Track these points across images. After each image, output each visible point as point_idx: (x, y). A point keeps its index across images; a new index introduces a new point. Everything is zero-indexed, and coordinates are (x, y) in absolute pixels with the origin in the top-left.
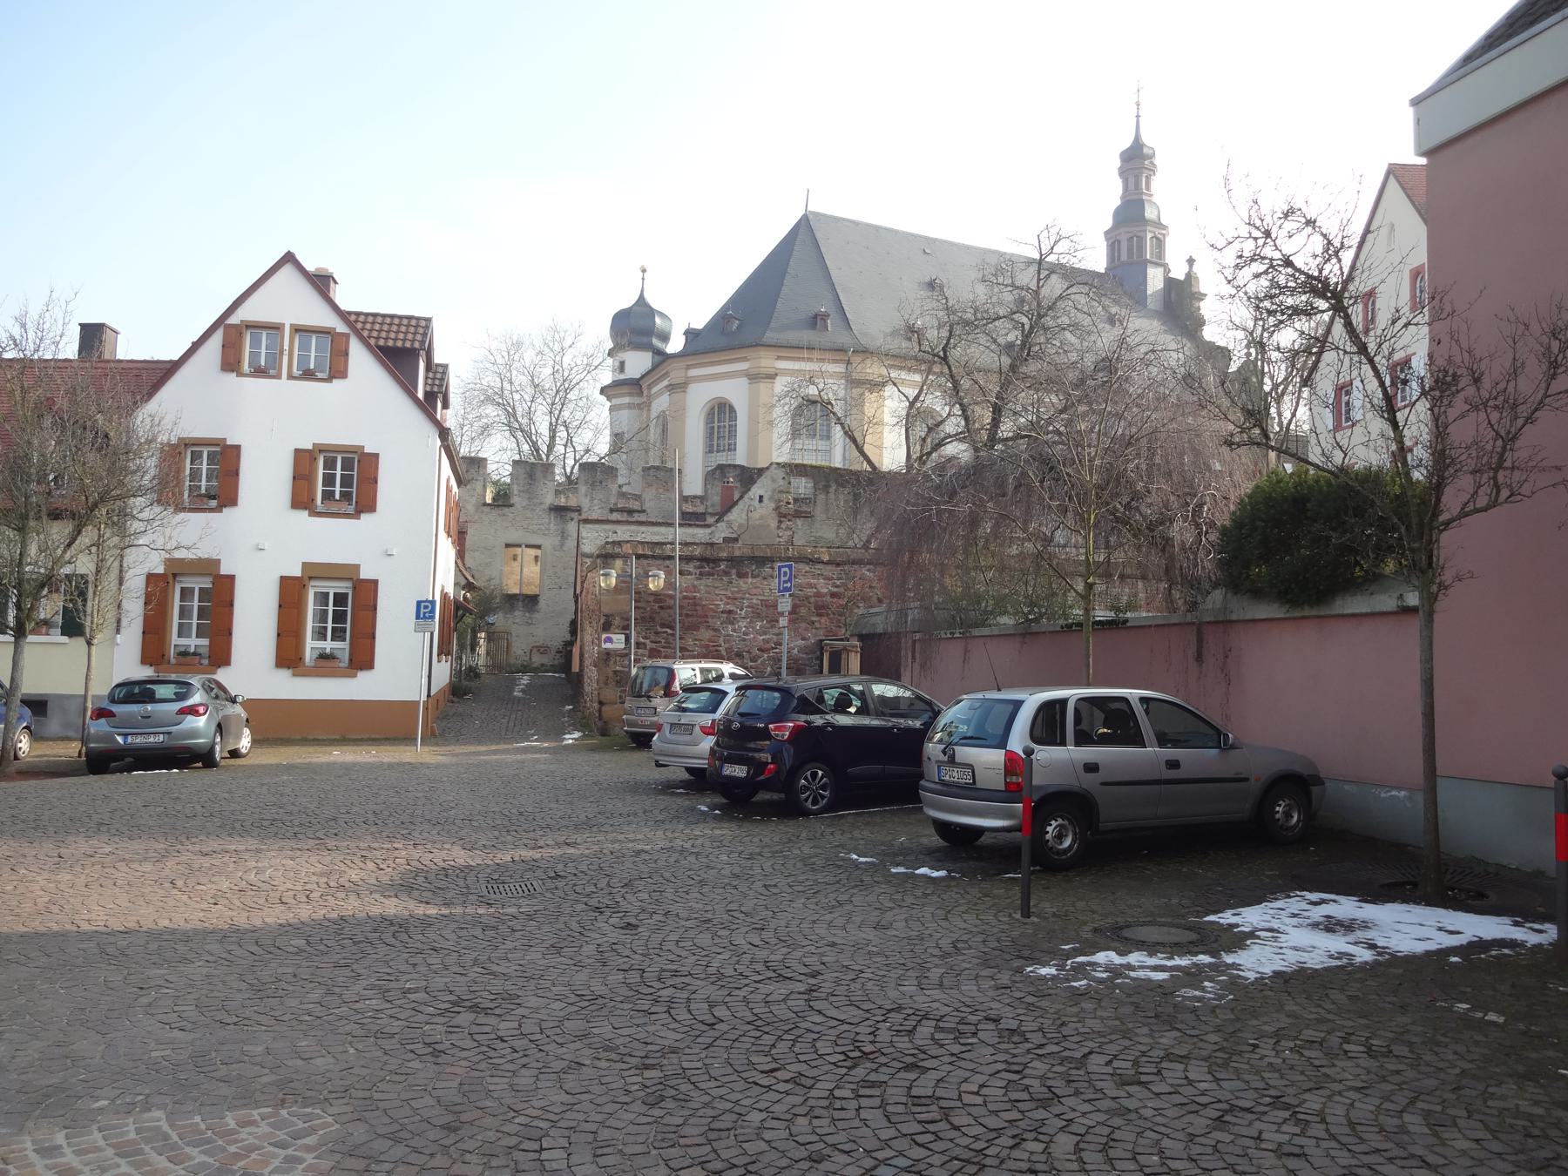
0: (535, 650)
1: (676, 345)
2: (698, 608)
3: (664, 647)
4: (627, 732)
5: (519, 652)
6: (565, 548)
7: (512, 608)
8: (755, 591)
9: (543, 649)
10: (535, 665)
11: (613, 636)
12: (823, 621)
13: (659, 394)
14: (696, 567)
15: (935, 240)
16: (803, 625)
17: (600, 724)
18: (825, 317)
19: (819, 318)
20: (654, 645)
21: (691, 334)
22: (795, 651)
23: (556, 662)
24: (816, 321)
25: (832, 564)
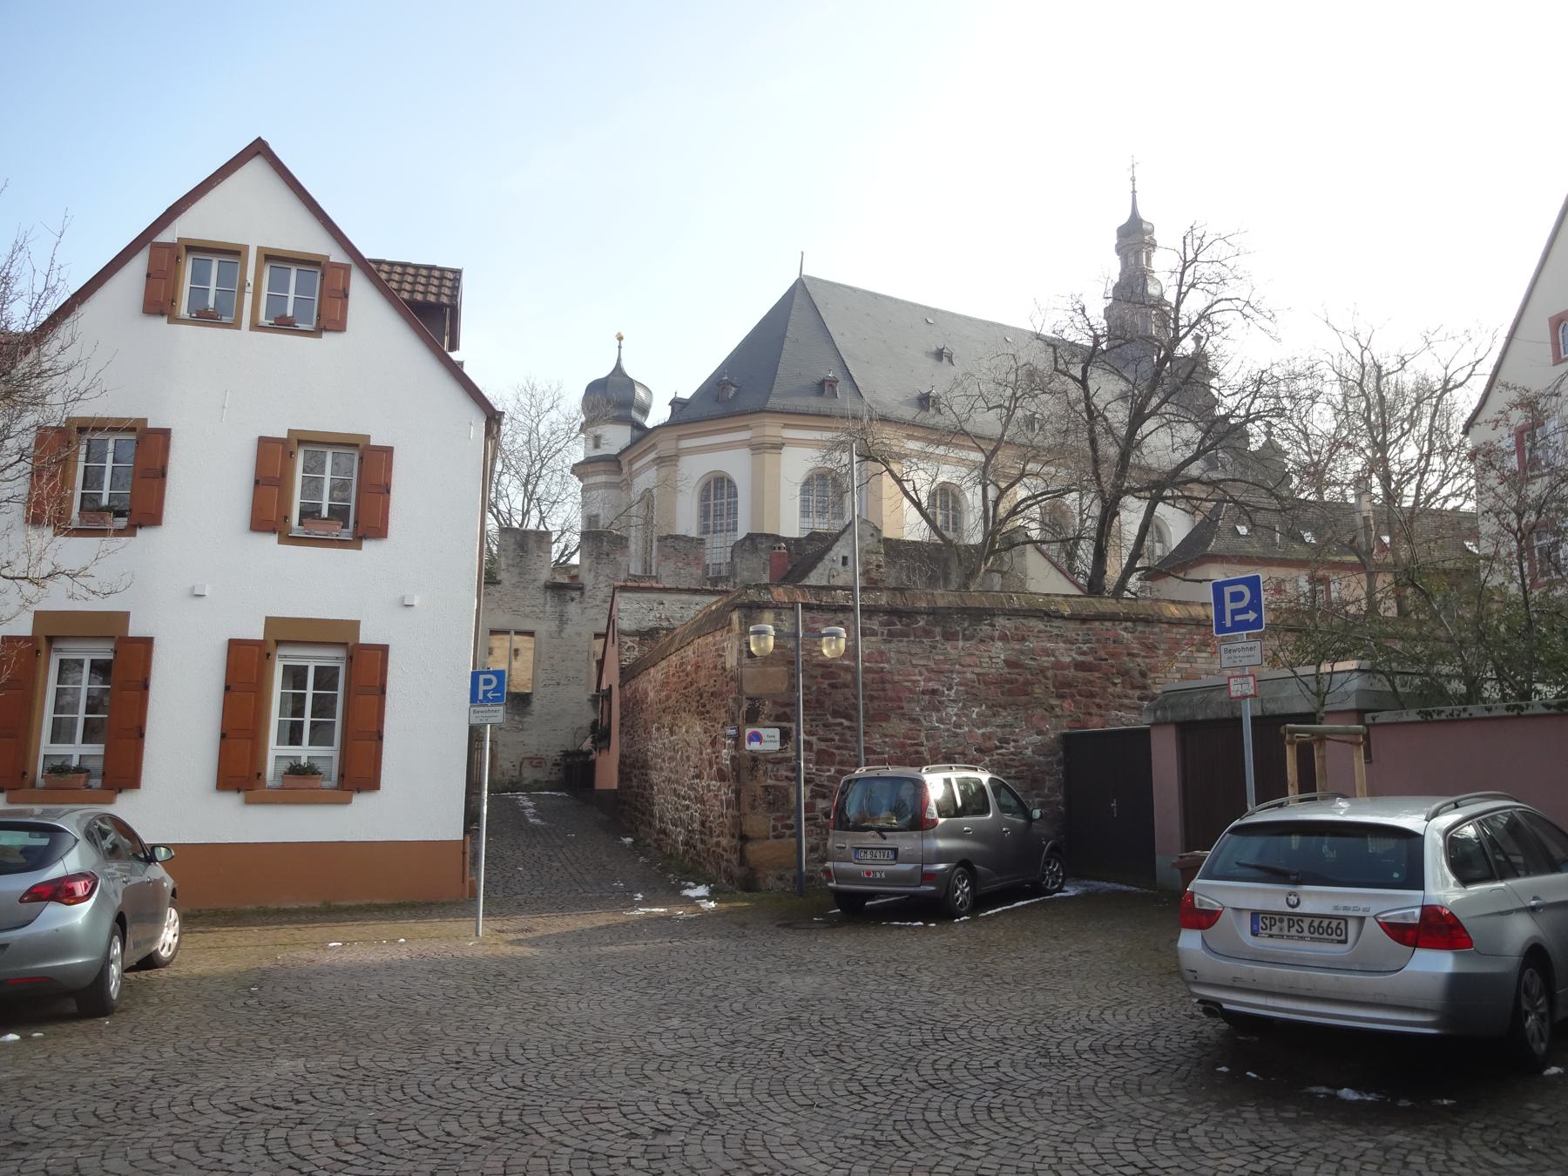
1: (658, 414)
2: (888, 686)
3: (838, 748)
4: (832, 890)
6: (563, 635)
8: (968, 660)
9: (536, 762)
10: (526, 782)
11: (761, 731)
12: (1066, 705)
13: (646, 467)
14: (882, 624)
15: (935, 311)
16: (1039, 711)
17: (738, 871)
18: (833, 383)
19: (827, 384)
20: (823, 745)
21: (676, 404)
22: (1029, 752)
23: (553, 778)
24: (824, 387)
25: (1076, 619)
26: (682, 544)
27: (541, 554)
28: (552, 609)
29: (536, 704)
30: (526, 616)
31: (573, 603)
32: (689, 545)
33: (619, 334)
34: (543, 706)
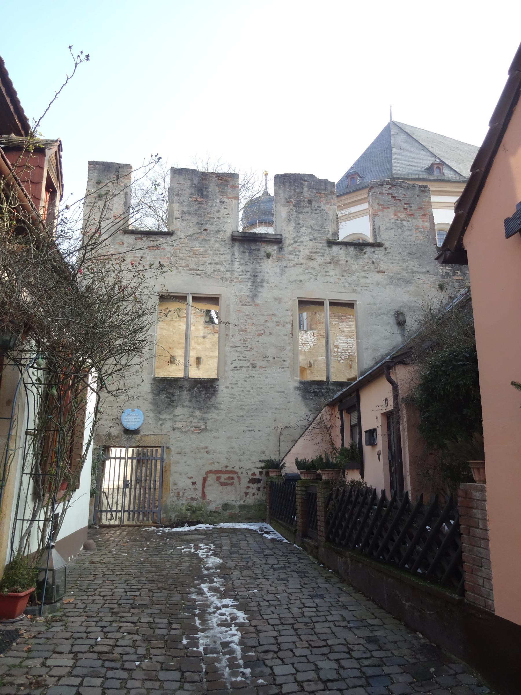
0: (211, 478)
5: (184, 483)
6: (258, 301)
7: (171, 403)
10: (212, 507)
19: (435, 167)
23: (250, 500)
26: (401, 191)
27: (225, 200)
28: (242, 268)
29: (222, 389)
30: (208, 276)
31: (270, 261)
32: (409, 193)
33: (265, 171)
34: (233, 397)
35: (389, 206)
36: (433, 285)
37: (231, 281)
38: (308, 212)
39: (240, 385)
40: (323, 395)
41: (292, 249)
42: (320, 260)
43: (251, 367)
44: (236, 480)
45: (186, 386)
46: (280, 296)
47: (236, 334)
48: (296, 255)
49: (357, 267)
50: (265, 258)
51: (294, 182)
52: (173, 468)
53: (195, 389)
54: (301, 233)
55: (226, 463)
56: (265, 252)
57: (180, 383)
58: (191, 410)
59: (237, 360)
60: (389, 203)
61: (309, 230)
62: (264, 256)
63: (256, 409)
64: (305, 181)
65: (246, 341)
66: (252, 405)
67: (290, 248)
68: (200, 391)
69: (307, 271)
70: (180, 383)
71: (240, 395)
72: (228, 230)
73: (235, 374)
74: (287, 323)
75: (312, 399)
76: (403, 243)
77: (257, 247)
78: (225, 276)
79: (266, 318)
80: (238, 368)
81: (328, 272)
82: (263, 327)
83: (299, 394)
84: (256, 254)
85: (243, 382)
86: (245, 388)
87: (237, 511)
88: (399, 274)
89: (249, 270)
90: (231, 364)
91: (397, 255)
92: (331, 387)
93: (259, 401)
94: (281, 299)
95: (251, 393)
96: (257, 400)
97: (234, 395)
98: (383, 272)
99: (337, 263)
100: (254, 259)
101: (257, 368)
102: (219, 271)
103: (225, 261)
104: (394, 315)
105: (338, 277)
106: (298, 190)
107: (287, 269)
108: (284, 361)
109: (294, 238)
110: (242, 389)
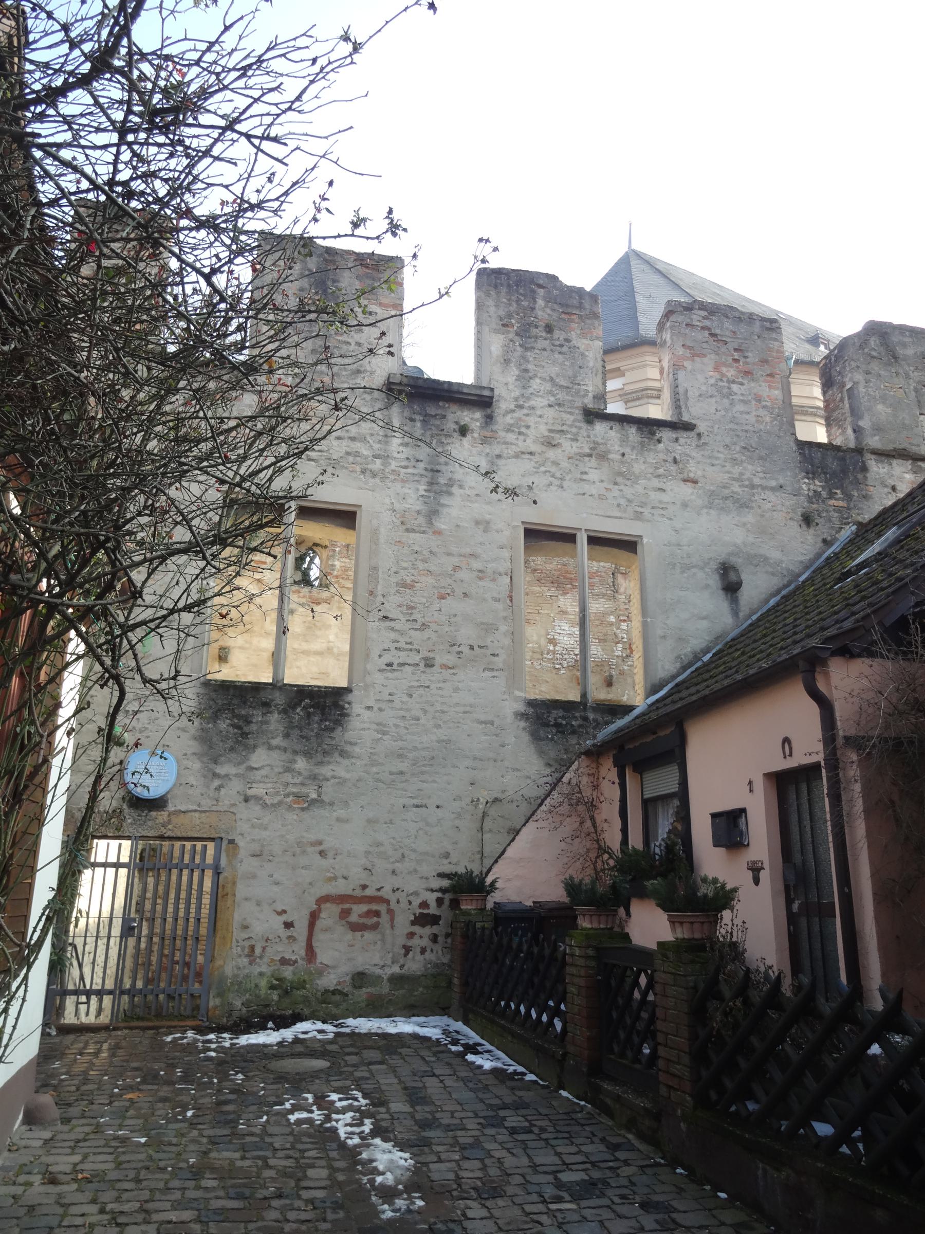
0: (329, 914)
10: (329, 981)
23: (415, 965)
26: (727, 324)
28: (407, 452)
31: (466, 441)
32: (743, 329)
34: (382, 729)
35: (705, 351)
36: (791, 515)
37: (384, 478)
38: (544, 350)
39: (397, 704)
40: (574, 732)
41: (512, 422)
42: (568, 447)
43: (422, 664)
44: (385, 918)
45: (278, 701)
46: (488, 517)
47: (393, 591)
48: (520, 433)
49: (643, 467)
50: (456, 435)
51: (517, 286)
52: (241, 890)
53: (298, 710)
54: (531, 390)
55: (363, 878)
56: (457, 423)
57: (264, 696)
58: (289, 755)
59: (392, 649)
60: (705, 345)
61: (548, 386)
62: (454, 431)
63: (433, 758)
64: (540, 286)
65: (413, 608)
66: (423, 749)
67: (509, 419)
68: (309, 715)
69: (543, 469)
70: (264, 696)
71: (396, 726)
72: (378, 372)
73: (387, 678)
74: (500, 574)
75: (552, 739)
76: (732, 426)
77: (439, 412)
78: (370, 466)
79: (455, 561)
80: (395, 667)
81: (586, 473)
82: (450, 581)
83: (524, 729)
84: (437, 427)
85: (405, 698)
86: (408, 710)
87: (385, 989)
88: (724, 487)
89: (421, 458)
90: (380, 656)
91: (721, 449)
92: (591, 716)
93: (438, 742)
94: (488, 523)
95: (422, 721)
96: (434, 738)
97: (385, 726)
98: (695, 482)
99: (603, 457)
100: (432, 436)
101: (436, 669)
102: (357, 454)
103: (372, 435)
104: (717, 570)
105: (605, 485)
106: (525, 303)
107: (501, 462)
108: (493, 655)
109: (516, 399)
110: (403, 713)
